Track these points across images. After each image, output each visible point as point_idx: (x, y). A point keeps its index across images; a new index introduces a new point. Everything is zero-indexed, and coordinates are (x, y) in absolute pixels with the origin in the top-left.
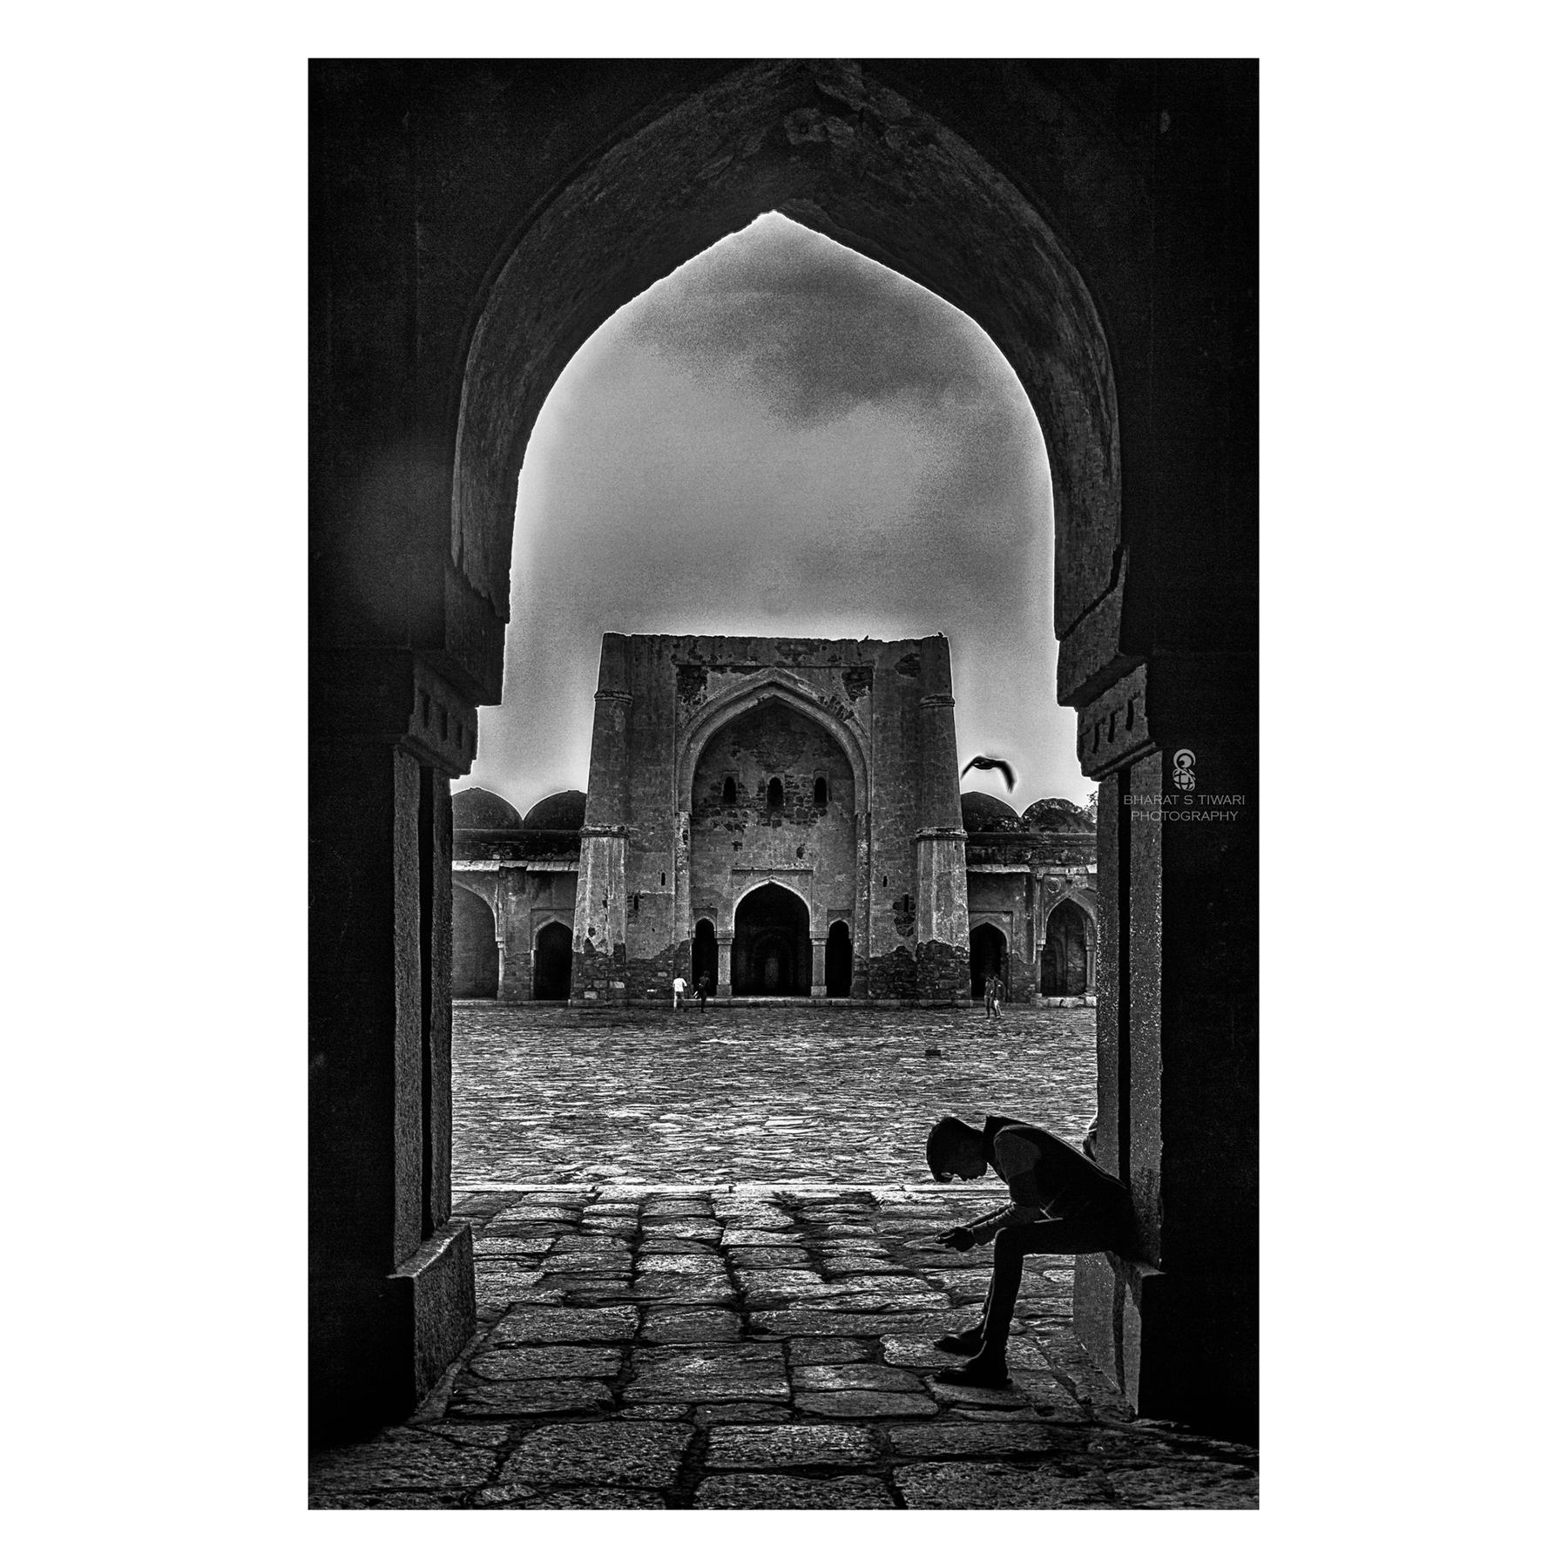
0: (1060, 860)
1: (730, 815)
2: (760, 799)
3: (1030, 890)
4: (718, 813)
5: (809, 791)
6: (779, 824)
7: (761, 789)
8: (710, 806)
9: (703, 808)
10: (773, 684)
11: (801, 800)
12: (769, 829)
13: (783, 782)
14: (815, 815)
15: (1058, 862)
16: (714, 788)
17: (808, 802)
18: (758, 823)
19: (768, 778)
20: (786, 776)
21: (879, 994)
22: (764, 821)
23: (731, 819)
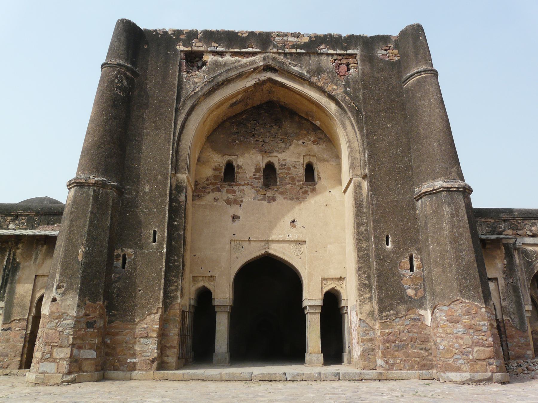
0: (531, 231)
1: (228, 192)
2: (256, 179)
3: (509, 256)
4: (219, 190)
5: (301, 171)
6: (274, 199)
7: (257, 170)
8: (212, 184)
9: (206, 185)
10: (267, 68)
11: (293, 179)
12: (265, 203)
13: (277, 166)
14: (306, 192)
15: (529, 233)
16: (216, 169)
17: (298, 181)
18: (254, 198)
19: (262, 161)
20: (279, 160)
21: (392, 365)
22: (259, 197)
23: (230, 196)
